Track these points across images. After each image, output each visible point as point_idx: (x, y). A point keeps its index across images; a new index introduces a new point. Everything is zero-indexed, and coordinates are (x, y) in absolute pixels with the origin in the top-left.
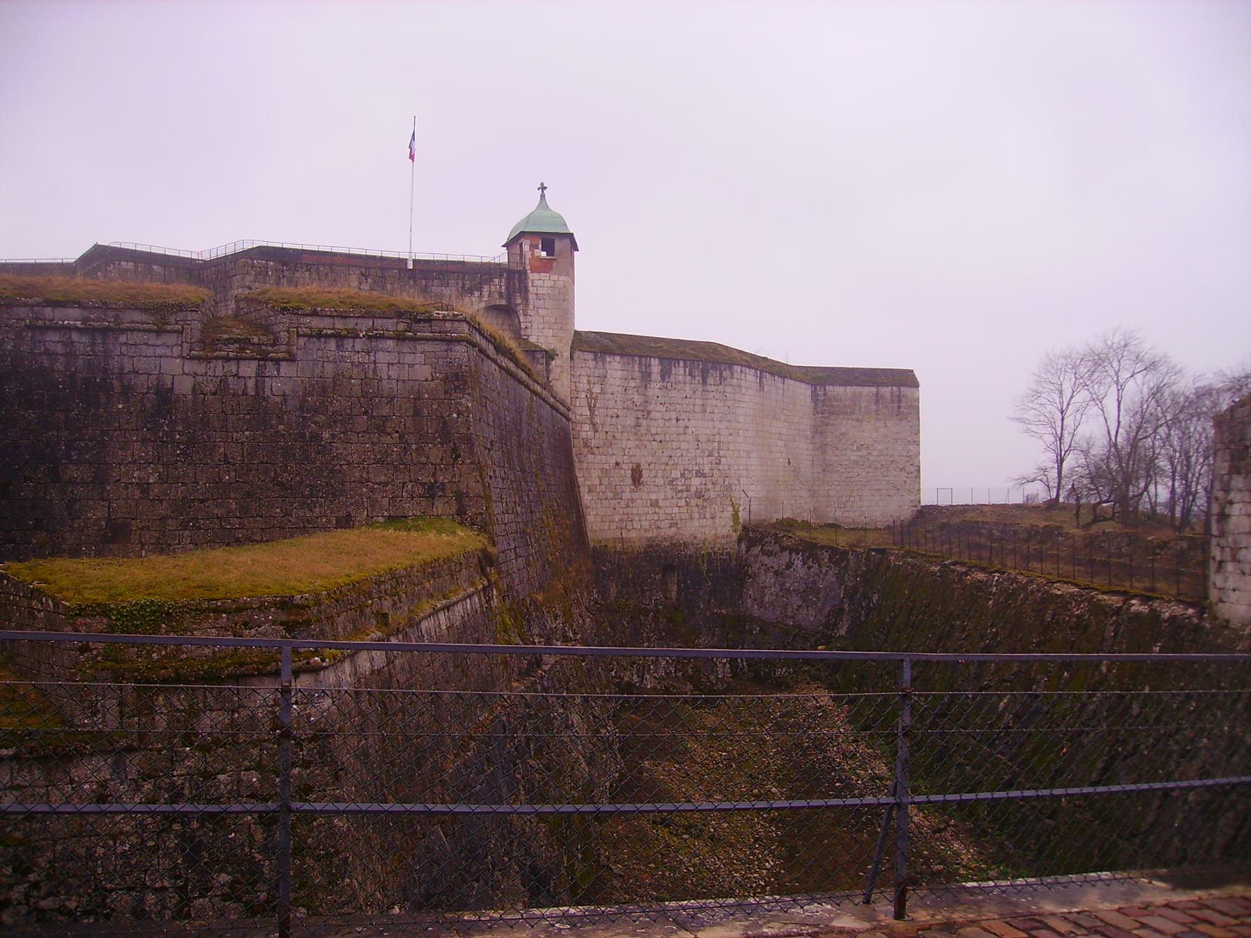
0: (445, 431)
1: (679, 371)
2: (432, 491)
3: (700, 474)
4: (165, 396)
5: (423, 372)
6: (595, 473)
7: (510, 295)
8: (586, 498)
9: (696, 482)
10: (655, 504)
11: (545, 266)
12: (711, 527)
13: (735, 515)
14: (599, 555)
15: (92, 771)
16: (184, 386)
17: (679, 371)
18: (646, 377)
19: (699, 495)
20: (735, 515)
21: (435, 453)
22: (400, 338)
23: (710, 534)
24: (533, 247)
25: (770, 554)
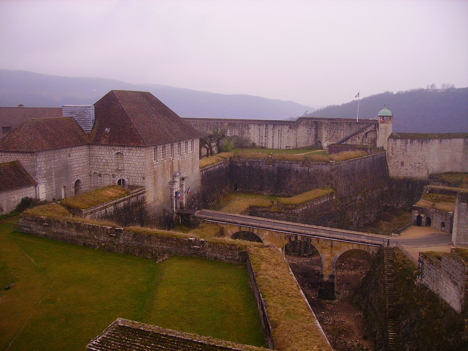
0: (331, 176)
1: (415, 142)
2: (328, 184)
3: (419, 163)
4: (297, 171)
5: (328, 169)
6: (392, 163)
7: (375, 128)
8: (390, 168)
9: (418, 165)
10: (407, 169)
11: (383, 122)
12: (422, 174)
13: (428, 172)
14: (392, 179)
15: (282, 214)
16: (300, 170)
17: (415, 142)
18: (407, 143)
19: (418, 168)
20: (428, 172)
21: (329, 179)
22: (325, 165)
23: (421, 176)
24: (381, 118)
25: (435, 181)
